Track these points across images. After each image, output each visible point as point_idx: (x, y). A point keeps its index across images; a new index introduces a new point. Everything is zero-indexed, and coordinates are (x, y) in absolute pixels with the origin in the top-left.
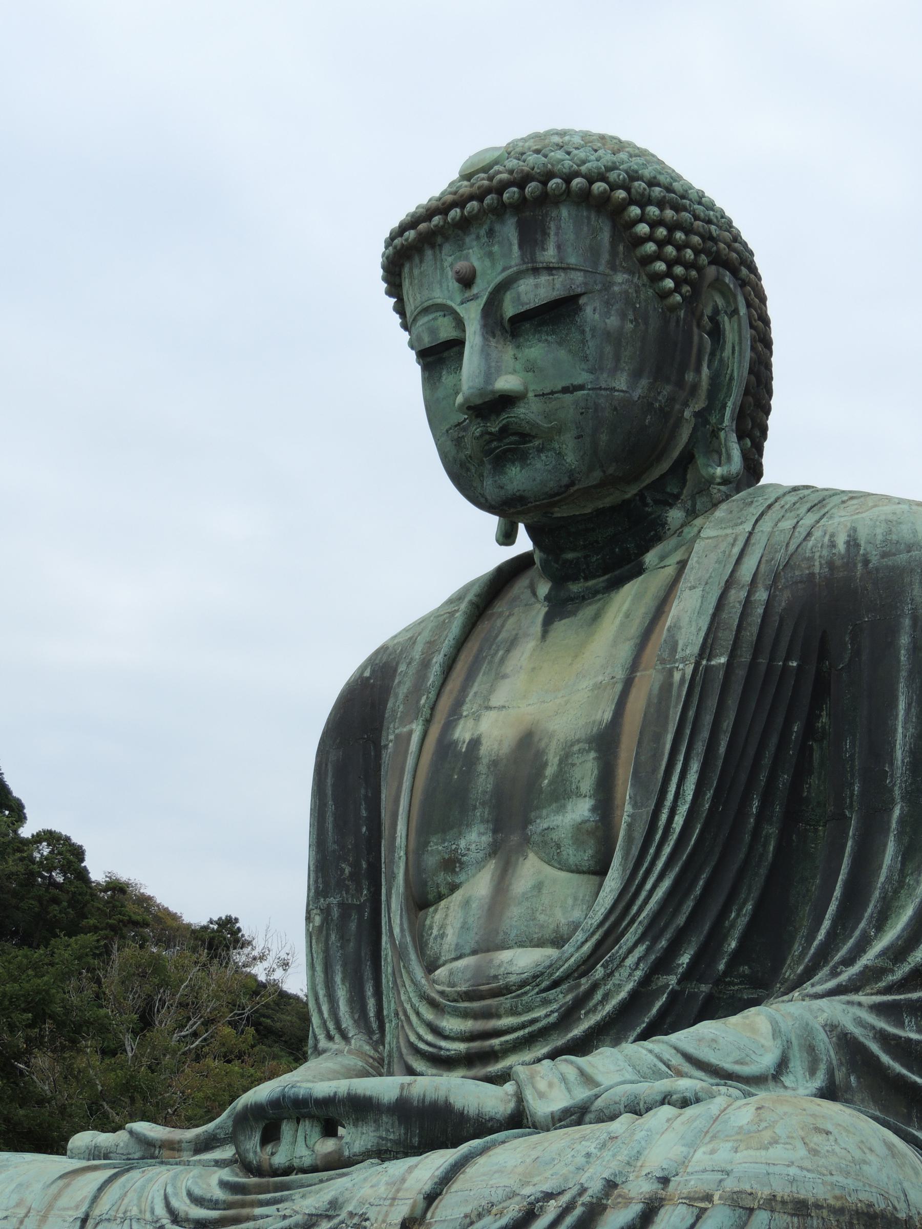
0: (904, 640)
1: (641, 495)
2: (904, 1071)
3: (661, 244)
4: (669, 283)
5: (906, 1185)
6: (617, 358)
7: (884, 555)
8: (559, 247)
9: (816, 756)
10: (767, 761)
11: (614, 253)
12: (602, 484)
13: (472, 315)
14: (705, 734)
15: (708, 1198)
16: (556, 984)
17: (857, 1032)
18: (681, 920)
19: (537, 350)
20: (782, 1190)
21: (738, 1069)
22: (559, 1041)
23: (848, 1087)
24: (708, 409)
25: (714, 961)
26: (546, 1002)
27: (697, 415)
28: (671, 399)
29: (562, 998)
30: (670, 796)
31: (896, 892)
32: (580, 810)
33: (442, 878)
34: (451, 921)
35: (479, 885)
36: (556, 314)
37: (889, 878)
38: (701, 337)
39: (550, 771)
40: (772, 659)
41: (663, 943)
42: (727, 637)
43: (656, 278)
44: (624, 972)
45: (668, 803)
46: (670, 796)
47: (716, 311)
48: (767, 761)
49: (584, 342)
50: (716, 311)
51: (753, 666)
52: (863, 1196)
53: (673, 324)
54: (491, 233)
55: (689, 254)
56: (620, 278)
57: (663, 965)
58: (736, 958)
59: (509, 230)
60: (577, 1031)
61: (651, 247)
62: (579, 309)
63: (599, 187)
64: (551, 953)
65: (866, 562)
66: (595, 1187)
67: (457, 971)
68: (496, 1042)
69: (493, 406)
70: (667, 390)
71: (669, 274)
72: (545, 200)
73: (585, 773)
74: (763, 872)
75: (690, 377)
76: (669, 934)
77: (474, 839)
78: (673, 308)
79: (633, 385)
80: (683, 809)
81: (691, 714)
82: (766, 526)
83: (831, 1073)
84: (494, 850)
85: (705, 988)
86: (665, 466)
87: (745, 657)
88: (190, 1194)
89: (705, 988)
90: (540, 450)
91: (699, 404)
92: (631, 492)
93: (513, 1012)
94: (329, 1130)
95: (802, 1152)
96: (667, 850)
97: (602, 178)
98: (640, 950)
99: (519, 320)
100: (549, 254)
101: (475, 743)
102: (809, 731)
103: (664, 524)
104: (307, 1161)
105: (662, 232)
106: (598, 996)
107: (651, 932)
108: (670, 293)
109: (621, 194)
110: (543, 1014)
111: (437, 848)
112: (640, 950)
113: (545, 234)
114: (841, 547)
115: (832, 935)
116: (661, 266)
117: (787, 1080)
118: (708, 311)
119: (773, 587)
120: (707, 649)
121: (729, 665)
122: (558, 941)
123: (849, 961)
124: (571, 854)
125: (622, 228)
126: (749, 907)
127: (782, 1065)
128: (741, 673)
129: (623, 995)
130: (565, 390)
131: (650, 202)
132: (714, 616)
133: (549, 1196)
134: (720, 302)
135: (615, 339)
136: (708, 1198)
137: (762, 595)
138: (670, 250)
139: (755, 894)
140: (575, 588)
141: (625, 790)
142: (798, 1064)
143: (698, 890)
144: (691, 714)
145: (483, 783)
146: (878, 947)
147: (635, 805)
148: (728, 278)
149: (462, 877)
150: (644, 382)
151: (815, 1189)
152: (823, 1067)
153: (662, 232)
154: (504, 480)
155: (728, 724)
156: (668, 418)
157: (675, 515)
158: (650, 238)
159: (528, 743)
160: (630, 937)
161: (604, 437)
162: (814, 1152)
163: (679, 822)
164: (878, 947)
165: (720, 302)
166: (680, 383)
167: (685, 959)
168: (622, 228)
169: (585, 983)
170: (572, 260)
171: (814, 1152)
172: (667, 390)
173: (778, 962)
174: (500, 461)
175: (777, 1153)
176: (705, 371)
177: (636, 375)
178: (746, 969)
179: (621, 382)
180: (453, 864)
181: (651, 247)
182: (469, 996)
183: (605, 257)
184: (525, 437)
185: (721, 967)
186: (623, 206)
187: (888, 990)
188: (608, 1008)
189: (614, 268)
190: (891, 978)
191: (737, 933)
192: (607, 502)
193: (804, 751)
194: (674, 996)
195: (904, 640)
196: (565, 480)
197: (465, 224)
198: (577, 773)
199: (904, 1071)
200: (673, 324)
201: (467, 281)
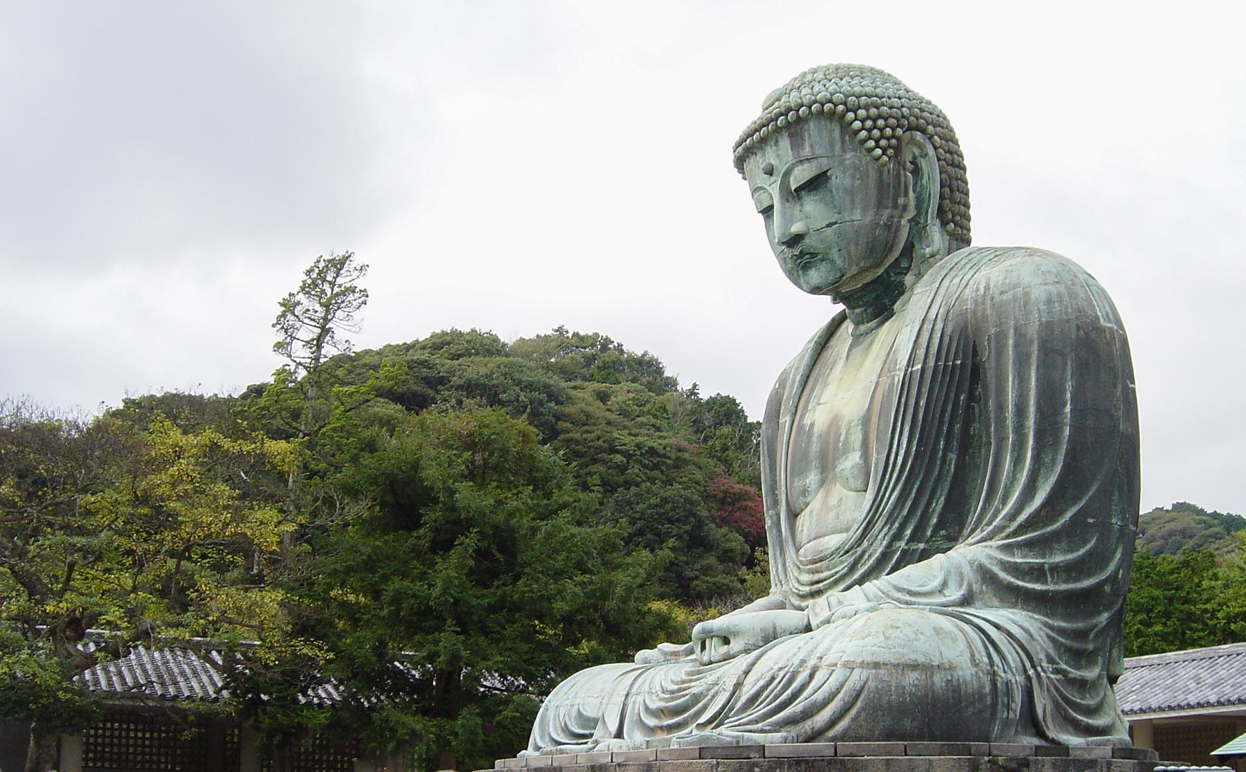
0: (1011, 342)
1: (886, 271)
2: (1013, 580)
3: (869, 131)
4: (878, 152)
5: (943, 648)
6: (853, 202)
7: (1002, 293)
8: (811, 147)
9: (977, 410)
10: (947, 419)
11: (843, 142)
12: (859, 273)
13: (775, 190)
14: (911, 410)
15: (836, 665)
16: (847, 552)
17: (986, 562)
18: (905, 512)
19: (812, 206)
20: (868, 659)
21: (919, 589)
22: (848, 582)
23: (981, 592)
24: (918, 214)
25: (924, 531)
26: (842, 562)
27: (909, 221)
29: (850, 559)
30: (895, 446)
31: (1012, 483)
32: (855, 457)
33: (801, 500)
34: (804, 522)
35: (816, 503)
36: (816, 183)
37: (1008, 476)
38: (906, 176)
39: (842, 438)
40: (946, 361)
41: (897, 525)
42: (921, 352)
43: (870, 150)
44: (878, 542)
45: (894, 450)
46: (895, 446)
47: (915, 157)
48: (947, 419)
49: (833, 197)
50: (915, 157)
51: (936, 367)
52: (913, 657)
53: (886, 173)
54: (777, 142)
55: (888, 131)
56: (848, 155)
57: (897, 536)
58: (937, 528)
59: (785, 142)
60: (856, 576)
61: (863, 134)
62: (829, 178)
63: (828, 106)
64: (845, 535)
65: (992, 299)
66: (797, 662)
67: (808, 550)
68: (821, 585)
69: (794, 241)
71: (877, 146)
72: (799, 120)
73: (856, 438)
74: (949, 480)
75: (901, 201)
76: (899, 520)
77: (813, 478)
78: (884, 165)
79: (864, 214)
80: (902, 452)
81: (903, 400)
82: (946, 283)
83: (970, 586)
84: (822, 482)
85: (922, 546)
86: (896, 253)
87: (931, 363)
88: (673, 682)
89: (922, 546)
90: (822, 260)
91: (911, 213)
92: (880, 271)
93: (829, 569)
94: (726, 641)
95: (882, 638)
96: (895, 475)
97: (830, 101)
98: (886, 529)
99: (798, 190)
100: (807, 152)
101: (812, 425)
102: (971, 397)
103: (902, 284)
104: (717, 658)
105: (869, 123)
106: (866, 556)
107: (890, 520)
108: (880, 157)
109: (841, 108)
110: (842, 568)
111: (798, 483)
112: (886, 529)
113: (803, 140)
114: (982, 290)
115: (984, 510)
116: (871, 143)
117: (946, 592)
118: (909, 158)
119: (945, 320)
120: (911, 362)
121: (923, 370)
122: (847, 530)
123: (988, 524)
124: (852, 482)
125: (845, 127)
126: (942, 499)
127: (944, 584)
128: (929, 373)
129: (877, 554)
130: (828, 226)
131: (859, 108)
132: (916, 341)
133: (781, 669)
134: (917, 151)
135: (850, 192)
136: (836, 665)
137: (939, 326)
138: (876, 133)
139: (945, 492)
140: (863, 328)
141: (873, 445)
142: (952, 584)
143: (913, 495)
144: (903, 400)
145: (815, 448)
146: (1003, 513)
147: (878, 453)
149: (809, 499)
150: (872, 212)
151: (885, 656)
152: (965, 584)
153: (869, 123)
154: (807, 279)
155: (922, 403)
156: (891, 228)
157: (908, 279)
158: (863, 128)
159: (835, 422)
160: (879, 524)
161: (853, 248)
162: (888, 638)
163: (900, 459)
164: (1003, 513)
165: (917, 151)
166: (895, 207)
167: (908, 532)
168: (845, 127)
169: (860, 550)
170: (819, 152)
171: (888, 638)
173: (962, 527)
174: (805, 268)
175: (870, 640)
176: (911, 194)
177: (864, 209)
178: (943, 532)
179: (857, 215)
180: (805, 492)
181: (863, 134)
182: (814, 562)
183: (838, 146)
184: (813, 255)
185: (929, 533)
186: (843, 116)
187: (1007, 537)
188: (871, 561)
189: (844, 151)
190: (1009, 530)
191: (936, 514)
192: (868, 280)
193: (968, 408)
194: (904, 552)
195: (1011, 342)
196: (839, 275)
197: (763, 141)
198: (853, 438)
199: (1013, 580)
200: (886, 173)
201: (770, 172)
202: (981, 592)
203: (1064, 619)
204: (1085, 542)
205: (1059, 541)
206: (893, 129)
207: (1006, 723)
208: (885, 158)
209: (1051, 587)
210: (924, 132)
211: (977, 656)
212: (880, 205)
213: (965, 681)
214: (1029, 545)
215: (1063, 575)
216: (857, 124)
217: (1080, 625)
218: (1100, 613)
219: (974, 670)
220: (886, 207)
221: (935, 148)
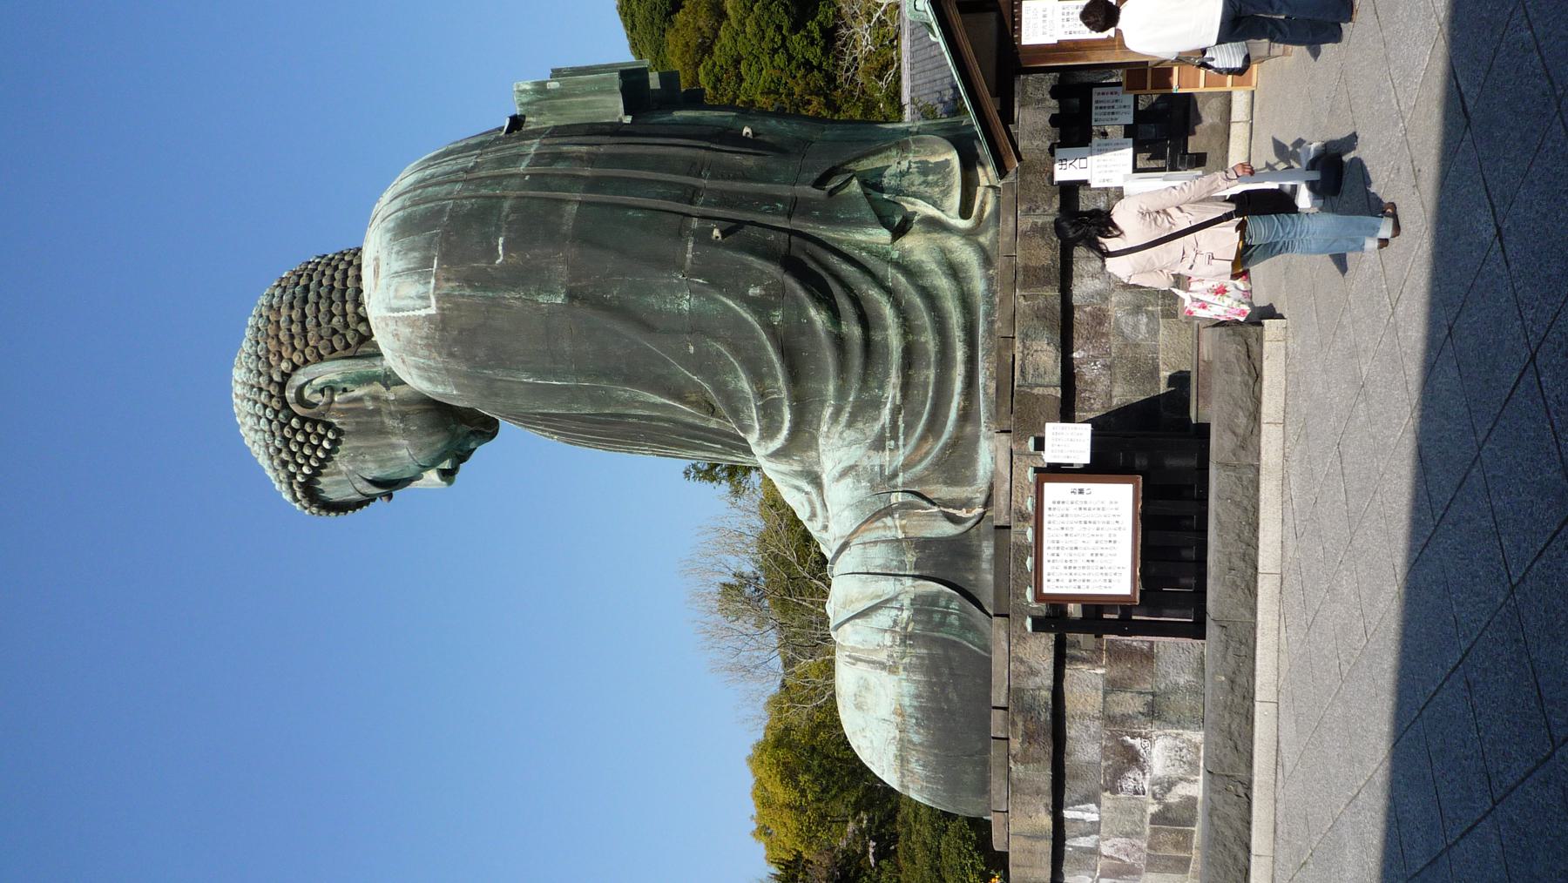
3: (307, 458)
4: (326, 444)
27: (388, 388)
28: (391, 414)
56: (343, 468)
70: (389, 422)
75: (370, 405)
91: (377, 388)
127: (798, 489)
148: (290, 394)
150: (394, 440)
166: (377, 412)
172: (389, 422)
176: (358, 392)
177: (393, 447)
179: (404, 453)
189: (340, 473)
202: (802, 461)
203: (826, 381)
204: (720, 354)
205: (725, 384)
206: (295, 431)
207: (967, 626)
208: (330, 435)
209: (784, 394)
210: (282, 387)
211: (882, 656)
212: (382, 432)
213: (917, 696)
214: (736, 413)
215: (768, 382)
216: (306, 470)
217: (829, 358)
218: (811, 322)
219: (903, 675)
220: (382, 423)
221: (295, 367)
